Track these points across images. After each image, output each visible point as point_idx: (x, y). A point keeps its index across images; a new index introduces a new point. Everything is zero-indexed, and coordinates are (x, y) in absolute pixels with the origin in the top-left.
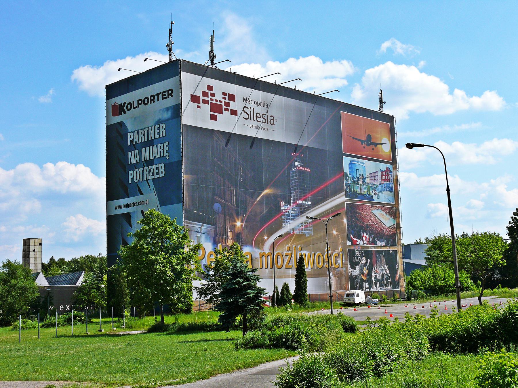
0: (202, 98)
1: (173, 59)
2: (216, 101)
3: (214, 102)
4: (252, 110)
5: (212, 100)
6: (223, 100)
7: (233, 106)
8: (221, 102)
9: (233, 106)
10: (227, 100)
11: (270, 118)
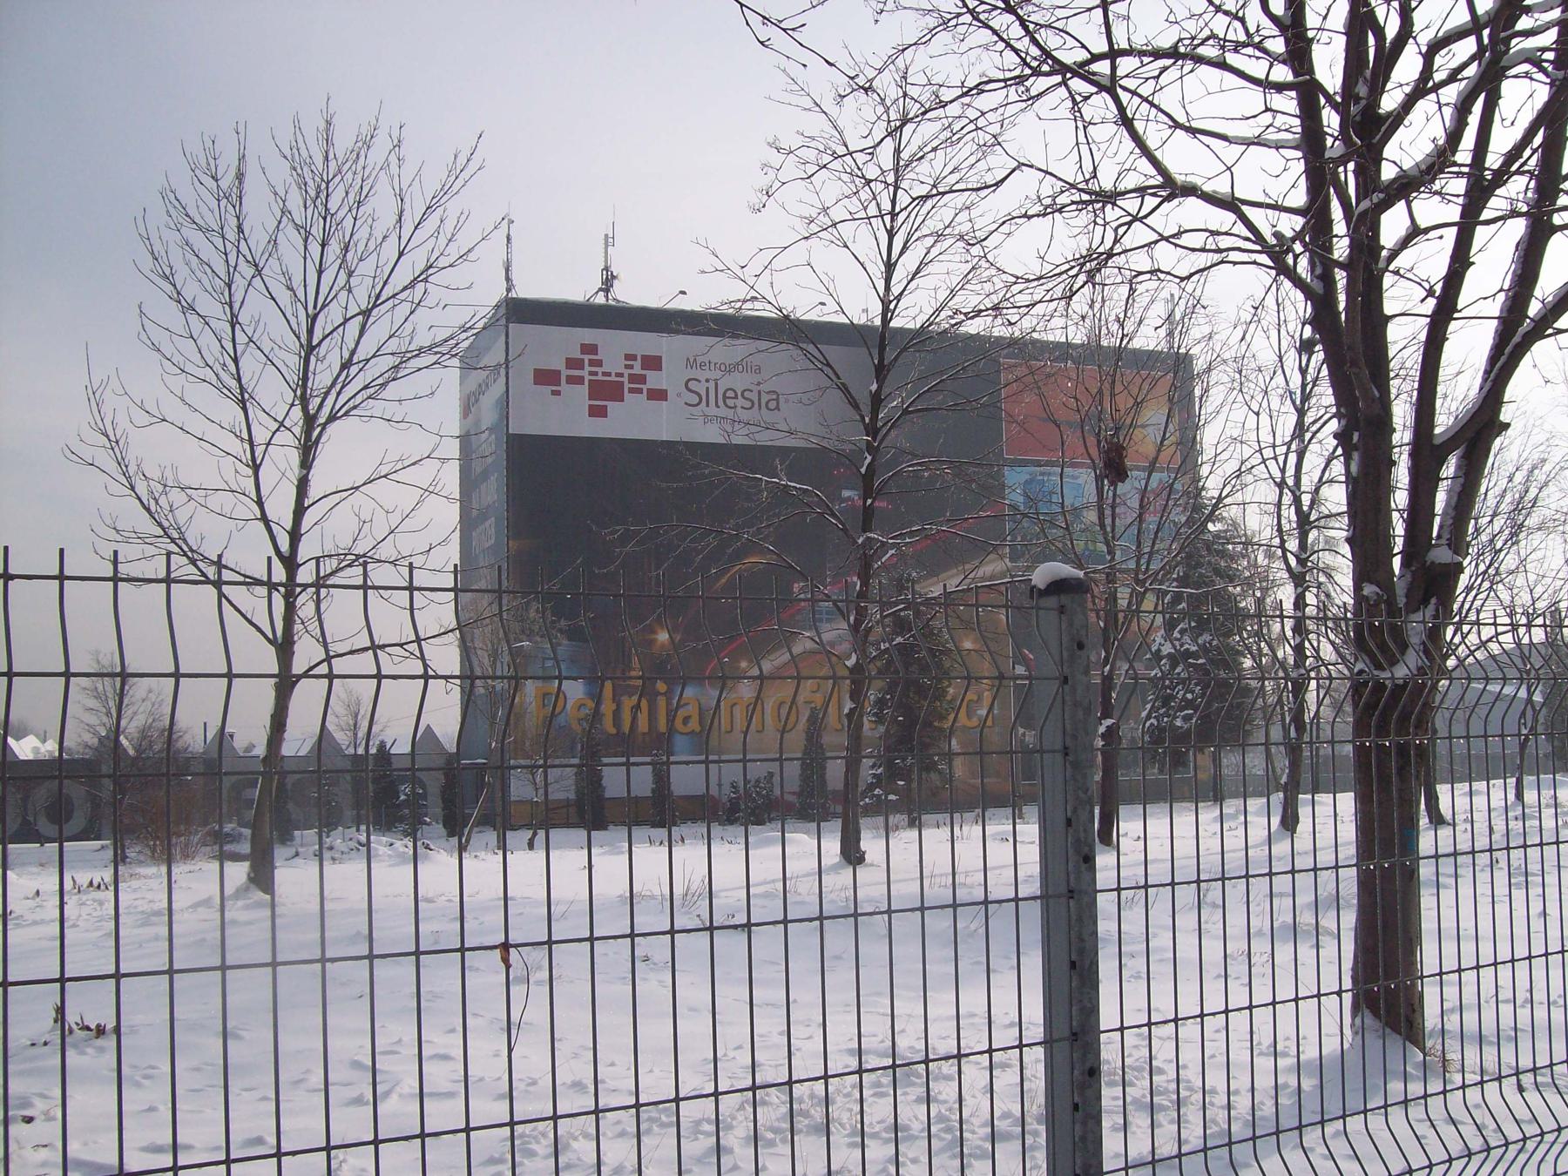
0: (565, 373)
1: (1343, 478)
2: (609, 374)
3: (600, 377)
4: (712, 385)
5: (591, 373)
6: (627, 372)
7: (654, 380)
8: (620, 375)
9: (654, 380)
10: (637, 370)
11: (765, 399)
